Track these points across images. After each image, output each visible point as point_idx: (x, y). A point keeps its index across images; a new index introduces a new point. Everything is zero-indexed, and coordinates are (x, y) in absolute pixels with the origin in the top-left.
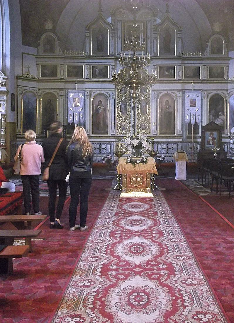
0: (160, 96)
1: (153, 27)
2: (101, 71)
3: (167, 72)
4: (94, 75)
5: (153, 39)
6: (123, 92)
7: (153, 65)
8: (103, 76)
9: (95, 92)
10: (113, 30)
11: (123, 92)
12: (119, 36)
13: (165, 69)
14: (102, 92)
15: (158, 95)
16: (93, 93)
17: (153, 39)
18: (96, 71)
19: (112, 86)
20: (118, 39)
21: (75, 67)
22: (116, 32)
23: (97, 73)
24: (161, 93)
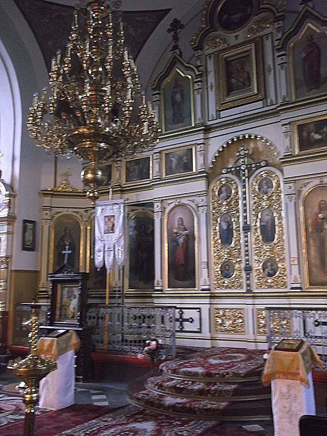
0: (303, 193)
1: (276, 43)
2: (180, 159)
3: (316, 133)
4: (169, 171)
5: (278, 67)
6: (224, 195)
7: (283, 125)
8: (184, 170)
9: (171, 203)
10: (199, 75)
11: (224, 195)
12: (211, 83)
13: (312, 127)
14: (184, 201)
15: (300, 192)
16: (169, 204)
17: (278, 67)
18: (171, 161)
19: (201, 185)
20: (209, 90)
21: (137, 162)
22: (204, 78)
23: (174, 166)
24: (305, 186)
